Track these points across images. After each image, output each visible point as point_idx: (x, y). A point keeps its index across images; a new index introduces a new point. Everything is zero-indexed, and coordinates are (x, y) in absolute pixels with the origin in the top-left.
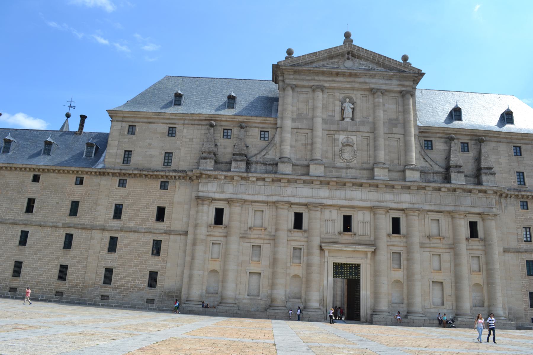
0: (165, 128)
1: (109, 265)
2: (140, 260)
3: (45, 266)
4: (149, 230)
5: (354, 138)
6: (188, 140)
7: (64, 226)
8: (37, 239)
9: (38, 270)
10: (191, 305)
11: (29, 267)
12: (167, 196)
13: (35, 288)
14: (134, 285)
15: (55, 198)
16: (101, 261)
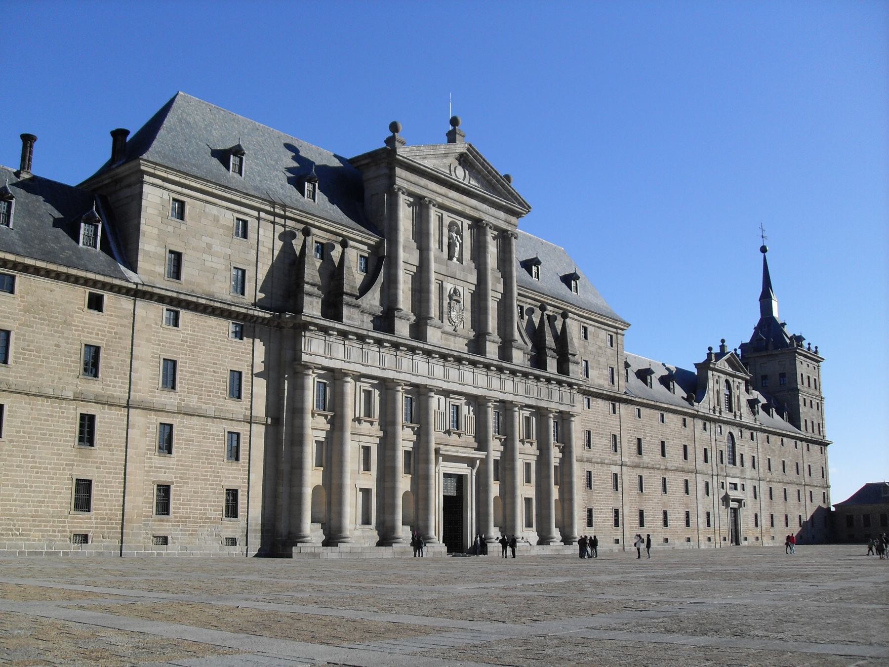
0: (228, 218)
1: (164, 478)
2: (211, 468)
3: (47, 483)
4: (223, 415)
5: (460, 289)
6: (266, 250)
7: (79, 398)
8: (22, 422)
9: (34, 492)
10: (308, 545)
11: (12, 486)
12: (242, 352)
13: (30, 530)
14: (205, 514)
15: (52, 335)
16: (147, 471)
